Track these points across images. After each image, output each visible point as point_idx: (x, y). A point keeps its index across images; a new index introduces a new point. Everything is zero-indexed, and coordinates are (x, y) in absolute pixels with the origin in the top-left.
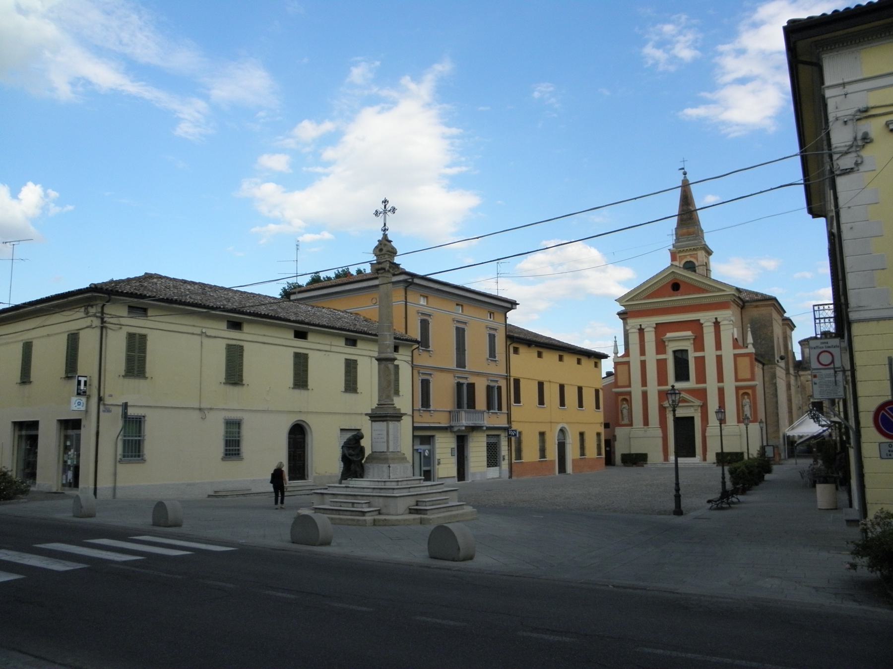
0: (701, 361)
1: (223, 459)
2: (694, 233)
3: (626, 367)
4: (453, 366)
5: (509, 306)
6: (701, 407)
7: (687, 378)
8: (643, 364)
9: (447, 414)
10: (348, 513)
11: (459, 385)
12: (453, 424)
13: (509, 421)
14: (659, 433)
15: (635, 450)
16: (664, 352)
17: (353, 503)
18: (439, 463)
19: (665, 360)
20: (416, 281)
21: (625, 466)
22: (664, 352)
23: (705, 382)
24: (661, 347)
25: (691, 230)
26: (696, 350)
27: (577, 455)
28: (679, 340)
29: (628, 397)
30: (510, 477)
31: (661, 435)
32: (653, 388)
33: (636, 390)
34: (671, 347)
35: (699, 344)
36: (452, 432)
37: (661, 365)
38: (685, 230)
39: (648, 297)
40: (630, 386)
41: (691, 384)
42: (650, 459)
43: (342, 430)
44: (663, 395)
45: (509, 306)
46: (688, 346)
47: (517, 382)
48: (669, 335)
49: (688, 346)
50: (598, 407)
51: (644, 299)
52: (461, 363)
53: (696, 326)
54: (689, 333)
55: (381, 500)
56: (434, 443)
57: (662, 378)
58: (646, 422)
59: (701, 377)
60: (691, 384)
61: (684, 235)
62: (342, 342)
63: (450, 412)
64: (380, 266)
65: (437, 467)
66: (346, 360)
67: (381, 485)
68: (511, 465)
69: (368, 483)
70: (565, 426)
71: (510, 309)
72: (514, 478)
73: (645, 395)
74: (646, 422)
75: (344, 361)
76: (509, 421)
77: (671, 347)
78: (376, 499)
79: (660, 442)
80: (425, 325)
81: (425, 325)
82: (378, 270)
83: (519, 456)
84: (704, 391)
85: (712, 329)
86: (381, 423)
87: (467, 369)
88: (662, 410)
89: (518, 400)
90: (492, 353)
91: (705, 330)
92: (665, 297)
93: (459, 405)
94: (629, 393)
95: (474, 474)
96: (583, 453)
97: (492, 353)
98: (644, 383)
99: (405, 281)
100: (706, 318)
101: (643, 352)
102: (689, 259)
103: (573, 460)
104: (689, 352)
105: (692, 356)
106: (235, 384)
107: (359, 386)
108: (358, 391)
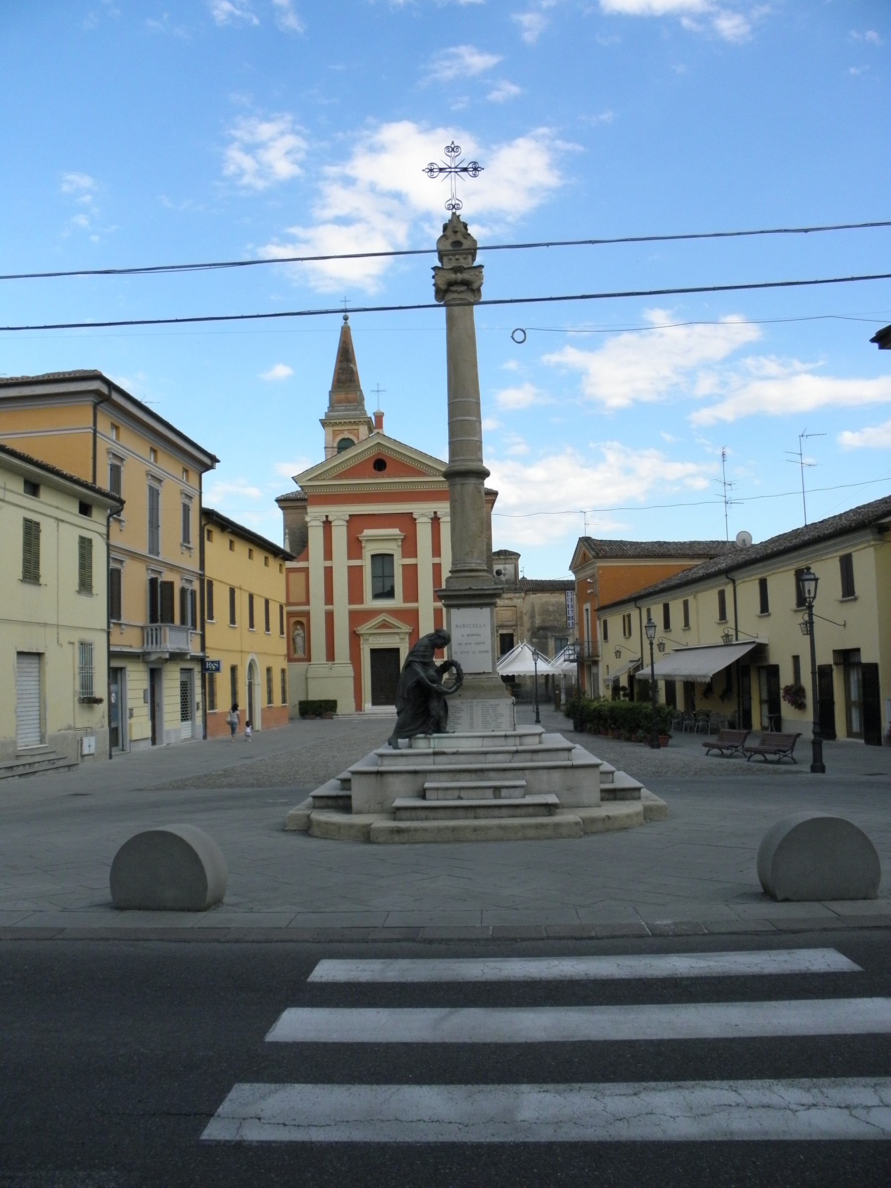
0: (411, 572)
1: (834, 651)
2: (355, 400)
3: (302, 576)
4: (145, 551)
5: (207, 461)
6: (410, 634)
7: (390, 594)
8: (329, 571)
9: (139, 631)
10: (461, 813)
11: (153, 582)
12: (149, 648)
13: (203, 648)
14: (350, 670)
15: (316, 695)
16: (360, 556)
17: (497, 789)
18: (131, 716)
19: (361, 567)
20: (115, 397)
21: (304, 719)
22: (360, 556)
23: (416, 600)
24: (355, 547)
25: (351, 396)
26: (404, 555)
27: (266, 705)
28: (381, 540)
29: (303, 620)
30: (205, 737)
31: (352, 674)
32: (342, 608)
33: (317, 609)
34: (370, 549)
35: (410, 546)
36: (146, 662)
37: (355, 574)
38: (342, 396)
39: (340, 476)
40: (307, 603)
41: (397, 602)
42: (340, 709)
43: (20, 654)
44: (356, 618)
45: (207, 461)
46: (393, 548)
47: (210, 583)
48: (367, 532)
49: (393, 548)
50: (282, 633)
51: (334, 478)
52: (154, 548)
53: (408, 521)
54: (396, 531)
55: (556, 775)
56: (123, 680)
57: (355, 595)
58: (331, 655)
59: (412, 593)
60: (397, 602)
61: (340, 402)
62: (20, 487)
63: (142, 628)
64: (459, 276)
65: (129, 721)
66: (26, 520)
67: (488, 745)
68: (205, 714)
69: (479, 742)
70: (255, 657)
71: (208, 468)
72: (209, 738)
73: (330, 616)
74: (331, 655)
75: (21, 523)
76: (203, 648)
77: (370, 549)
78: (544, 775)
79: (351, 683)
80: (116, 472)
81: (116, 472)
82: (451, 284)
83: (212, 707)
84: (416, 612)
85: (429, 527)
86: (477, 610)
87: (160, 558)
88: (355, 638)
89: (211, 617)
90: (186, 538)
91: (419, 528)
92: (365, 478)
93: (153, 619)
94: (307, 614)
95: (168, 732)
96: (270, 701)
97: (186, 538)
98: (329, 598)
99: (97, 392)
100: (422, 511)
101: (328, 554)
102: (346, 435)
103: (263, 710)
104: (395, 558)
105: (399, 562)
106: (85, 514)
107: (42, 571)
108: (42, 580)
